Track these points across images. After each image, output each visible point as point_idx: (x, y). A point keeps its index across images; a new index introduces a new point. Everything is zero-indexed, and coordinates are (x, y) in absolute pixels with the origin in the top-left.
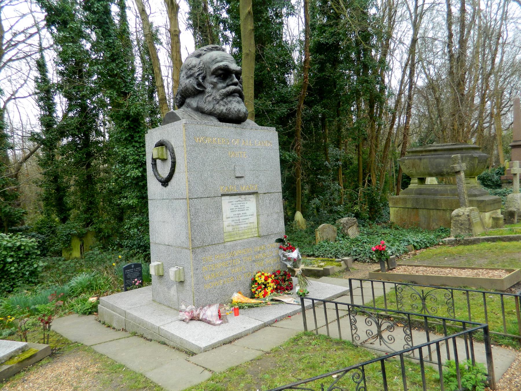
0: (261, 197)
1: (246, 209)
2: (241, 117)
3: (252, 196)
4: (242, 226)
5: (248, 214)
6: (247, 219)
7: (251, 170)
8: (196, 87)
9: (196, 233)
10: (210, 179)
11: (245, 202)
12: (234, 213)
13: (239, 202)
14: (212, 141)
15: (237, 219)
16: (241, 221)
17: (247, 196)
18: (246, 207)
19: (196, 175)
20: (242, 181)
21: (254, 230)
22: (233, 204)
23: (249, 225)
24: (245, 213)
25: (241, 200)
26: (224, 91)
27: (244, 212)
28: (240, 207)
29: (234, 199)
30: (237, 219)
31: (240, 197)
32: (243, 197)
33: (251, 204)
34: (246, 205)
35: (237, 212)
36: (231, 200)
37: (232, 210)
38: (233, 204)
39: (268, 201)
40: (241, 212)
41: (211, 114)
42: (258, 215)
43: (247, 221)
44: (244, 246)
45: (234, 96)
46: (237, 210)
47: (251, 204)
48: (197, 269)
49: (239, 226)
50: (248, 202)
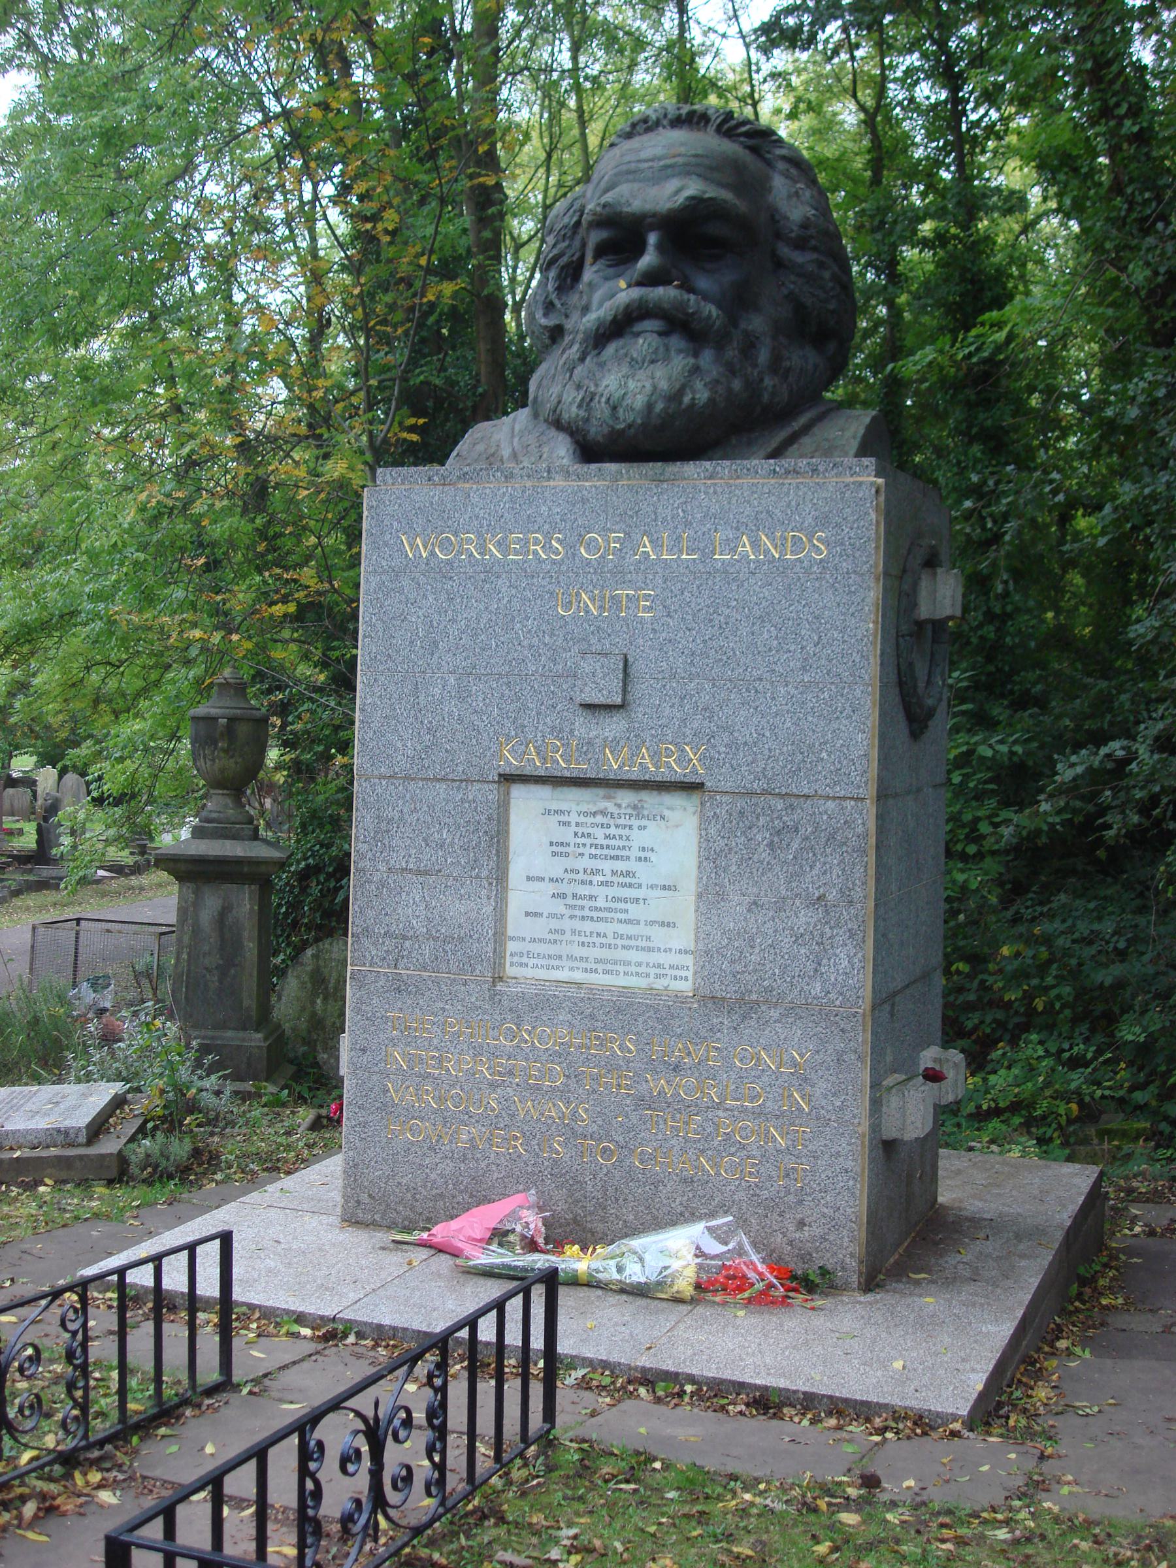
0: (722, 812)
1: (635, 853)
7: (673, 676)
8: (539, 315)
9: (371, 913)
10: (452, 707)
11: (636, 823)
12: (569, 863)
13: (599, 819)
14: (483, 550)
15: (584, 890)
16: (601, 903)
17: (650, 800)
18: (635, 845)
19: (393, 687)
20: (613, 726)
24: (628, 874)
26: (591, 319)
27: (620, 866)
28: (601, 841)
29: (574, 801)
30: (584, 890)
31: (608, 798)
32: (626, 798)
33: (671, 840)
34: (639, 838)
35: (584, 863)
36: (554, 806)
37: (559, 849)
40: (607, 866)
41: (558, 424)
43: (634, 911)
44: (592, 1017)
45: (638, 335)
46: (587, 851)
48: (364, 1050)
49: (588, 926)
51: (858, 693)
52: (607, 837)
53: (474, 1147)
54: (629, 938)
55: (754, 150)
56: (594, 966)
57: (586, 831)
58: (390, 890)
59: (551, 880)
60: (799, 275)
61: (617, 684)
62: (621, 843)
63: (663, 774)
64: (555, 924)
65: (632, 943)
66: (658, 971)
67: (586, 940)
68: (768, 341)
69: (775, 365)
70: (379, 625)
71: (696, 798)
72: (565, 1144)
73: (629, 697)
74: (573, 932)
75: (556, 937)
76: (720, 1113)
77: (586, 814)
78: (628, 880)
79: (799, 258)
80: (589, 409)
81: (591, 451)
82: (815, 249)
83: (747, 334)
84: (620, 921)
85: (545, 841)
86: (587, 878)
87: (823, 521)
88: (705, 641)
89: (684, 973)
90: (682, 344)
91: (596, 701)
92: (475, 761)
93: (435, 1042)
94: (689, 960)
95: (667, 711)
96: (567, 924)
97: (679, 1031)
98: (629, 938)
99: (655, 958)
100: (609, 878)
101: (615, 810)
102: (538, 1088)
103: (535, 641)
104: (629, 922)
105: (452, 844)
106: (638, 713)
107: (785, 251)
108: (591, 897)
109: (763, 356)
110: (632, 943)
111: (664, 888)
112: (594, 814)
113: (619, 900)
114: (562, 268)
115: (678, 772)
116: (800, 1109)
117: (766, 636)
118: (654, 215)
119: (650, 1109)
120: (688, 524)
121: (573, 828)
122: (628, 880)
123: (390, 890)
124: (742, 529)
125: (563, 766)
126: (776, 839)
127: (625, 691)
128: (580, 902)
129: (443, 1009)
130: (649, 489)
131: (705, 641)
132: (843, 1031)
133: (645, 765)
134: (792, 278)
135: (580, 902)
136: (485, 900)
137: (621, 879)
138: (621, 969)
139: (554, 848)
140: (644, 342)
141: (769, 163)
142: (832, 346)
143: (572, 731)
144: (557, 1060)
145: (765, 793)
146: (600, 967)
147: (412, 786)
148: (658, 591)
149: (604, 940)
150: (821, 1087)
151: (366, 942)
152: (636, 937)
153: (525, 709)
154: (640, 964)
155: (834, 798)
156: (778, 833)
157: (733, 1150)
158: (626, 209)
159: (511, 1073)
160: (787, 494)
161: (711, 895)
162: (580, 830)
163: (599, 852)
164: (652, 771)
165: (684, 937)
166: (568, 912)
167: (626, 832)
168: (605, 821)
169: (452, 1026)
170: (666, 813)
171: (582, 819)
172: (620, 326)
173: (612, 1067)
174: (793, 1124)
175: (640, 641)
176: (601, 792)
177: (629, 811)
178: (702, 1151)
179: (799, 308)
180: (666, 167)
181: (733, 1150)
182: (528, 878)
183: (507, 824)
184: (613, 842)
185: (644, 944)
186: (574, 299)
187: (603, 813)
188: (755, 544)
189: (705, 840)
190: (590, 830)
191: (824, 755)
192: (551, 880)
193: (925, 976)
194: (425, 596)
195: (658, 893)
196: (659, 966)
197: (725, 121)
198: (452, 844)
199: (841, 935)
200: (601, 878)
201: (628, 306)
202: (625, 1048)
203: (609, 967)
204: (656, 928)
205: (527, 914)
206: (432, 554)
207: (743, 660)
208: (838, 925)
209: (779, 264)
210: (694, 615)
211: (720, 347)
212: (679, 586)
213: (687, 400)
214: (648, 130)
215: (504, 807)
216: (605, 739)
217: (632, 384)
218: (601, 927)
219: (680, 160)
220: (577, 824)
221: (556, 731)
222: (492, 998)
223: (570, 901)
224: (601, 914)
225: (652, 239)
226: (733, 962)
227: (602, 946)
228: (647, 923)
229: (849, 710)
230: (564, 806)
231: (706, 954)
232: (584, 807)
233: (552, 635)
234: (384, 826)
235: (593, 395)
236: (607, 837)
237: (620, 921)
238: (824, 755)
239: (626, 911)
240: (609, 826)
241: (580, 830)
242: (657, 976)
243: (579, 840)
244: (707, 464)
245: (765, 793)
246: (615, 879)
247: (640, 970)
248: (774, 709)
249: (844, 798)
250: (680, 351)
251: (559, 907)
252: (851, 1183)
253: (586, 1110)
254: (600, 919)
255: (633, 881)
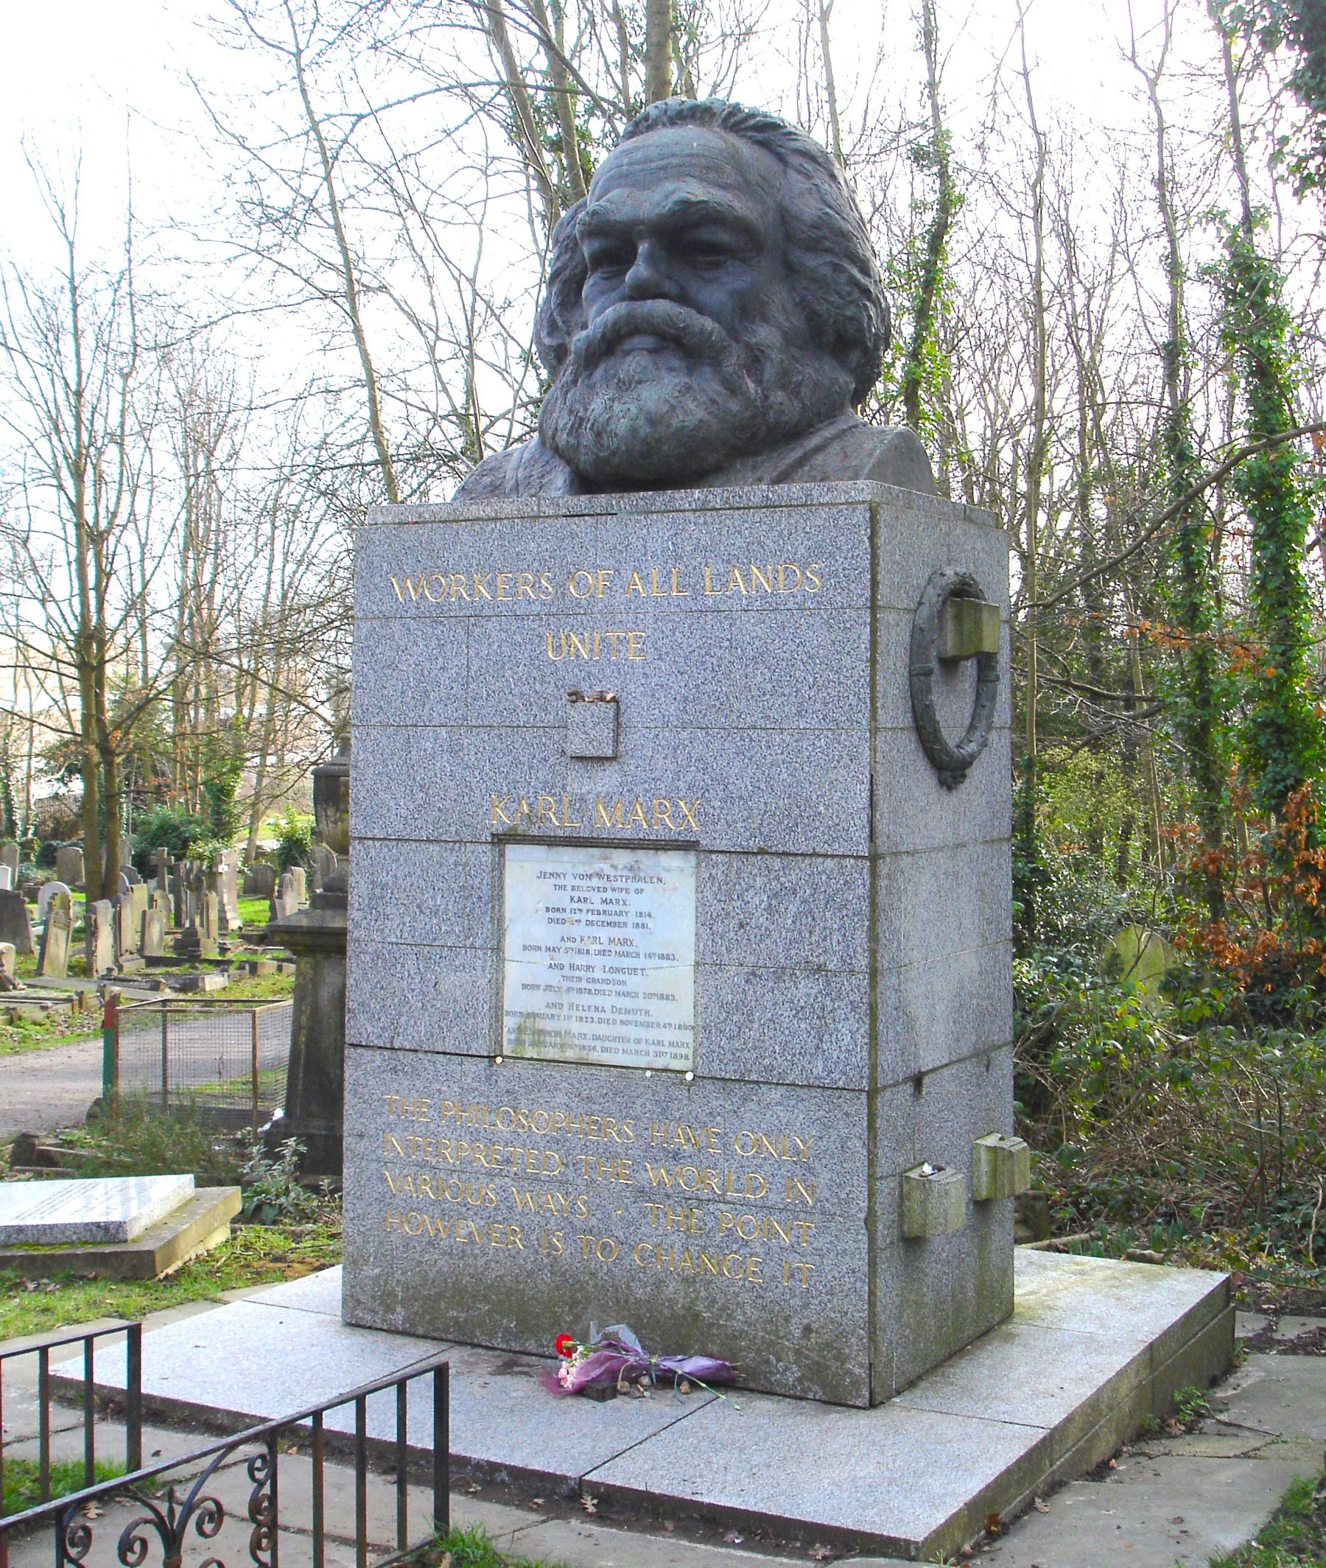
1: (632, 919)
2: (606, 461)
3: (672, 861)
4: (607, 1002)
5: (641, 950)
6: (634, 971)
10: (444, 762)
11: (632, 886)
12: (566, 930)
13: (595, 882)
14: (471, 588)
15: (581, 961)
16: (598, 974)
18: (632, 909)
19: (385, 741)
20: (607, 779)
21: (668, 1035)
22: (563, 888)
23: (640, 1003)
24: (625, 942)
25: (607, 870)
27: (617, 933)
30: (581, 961)
31: (606, 858)
32: (622, 858)
34: (637, 903)
37: (555, 915)
38: (563, 888)
39: (758, 900)
40: (604, 933)
42: (697, 963)
43: (634, 982)
44: (589, 1099)
45: (627, 353)
46: (583, 917)
47: (670, 901)
48: (361, 1136)
49: (585, 1000)
50: (648, 888)
51: (855, 740)
52: (605, 901)
53: (473, 1242)
54: (627, 1012)
55: (764, 144)
56: (592, 1043)
57: (582, 895)
58: (384, 960)
59: (548, 949)
60: (813, 280)
61: (608, 734)
62: (618, 908)
63: (657, 833)
64: (551, 997)
65: (631, 1017)
66: (658, 1049)
67: (584, 1014)
68: (776, 355)
69: (784, 380)
70: (371, 676)
71: (692, 857)
72: (564, 1239)
73: (621, 748)
74: (571, 1005)
75: (553, 1011)
76: (721, 1206)
77: (582, 877)
78: (626, 949)
79: (811, 261)
80: (578, 437)
81: (585, 483)
82: (828, 250)
83: (748, 346)
84: (618, 994)
85: (542, 906)
86: (582, 946)
87: (816, 552)
88: (697, 686)
89: (684, 1051)
90: (675, 362)
91: (587, 754)
92: (468, 820)
93: (432, 1126)
94: (688, 1037)
95: (661, 762)
96: (565, 999)
97: (677, 1115)
98: (627, 1012)
99: (652, 1034)
100: (606, 947)
101: (612, 872)
102: (536, 1179)
103: (526, 689)
104: (627, 994)
105: (446, 910)
106: (631, 764)
107: (796, 255)
108: (588, 967)
109: (769, 373)
110: (631, 1017)
111: (662, 957)
112: (590, 877)
113: (618, 970)
114: (565, 283)
115: (669, 827)
116: (805, 1203)
117: (759, 679)
118: (642, 222)
119: (650, 1201)
120: (678, 558)
121: (569, 892)
122: (626, 949)
123: (384, 960)
124: (734, 562)
125: (555, 825)
126: (774, 902)
127: (616, 741)
128: (577, 973)
129: (440, 1091)
130: (638, 521)
131: (697, 686)
132: (847, 1114)
133: (638, 823)
134: (805, 283)
135: (577, 973)
136: (479, 973)
137: (619, 948)
138: (620, 1046)
139: (551, 915)
140: (633, 363)
141: (781, 158)
142: (855, 357)
143: (564, 787)
144: (555, 1146)
145: (762, 852)
146: (599, 1044)
147: (405, 847)
148: (649, 632)
149: (602, 1015)
150: (824, 1177)
151: (362, 1017)
152: (634, 1012)
153: (517, 763)
154: (638, 1041)
155: (833, 856)
156: (776, 895)
157: (735, 1247)
158: (618, 217)
159: (508, 1161)
160: (779, 523)
161: (707, 965)
162: (576, 894)
163: (595, 918)
164: (644, 831)
165: (684, 1010)
166: (566, 984)
167: (623, 895)
168: (601, 883)
169: (447, 1109)
170: (663, 875)
171: (578, 882)
172: (609, 345)
173: (610, 1155)
174: (796, 1218)
175: (632, 686)
176: (595, 851)
177: (626, 873)
178: (704, 1248)
179: (812, 317)
180: (659, 169)
181: (735, 1247)
182: (525, 948)
183: (502, 889)
184: (609, 907)
185: (643, 1018)
186: (576, 317)
187: (599, 875)
188: (747, 577)
189: (701, 903)
190: (587, 895)
191: (822, 808)
192: (548, 949)
193: (983, 1056)
194: (416, 643)
195: (656, 962)
196: (660, 1043)
197: (730, 114)
198: (446, 910)
199: (842, 1007)
200: (598, 947)
201: (615, 324)
202: (622, 1134)
203: (607, 1044)
204: (655, 1001)
205: (525, 986)
206: (423, 597)
207: (737, 705)
208: (839, 998)
209: (791, 270)
210: (686, 658)
211: (716, 363)
212: (670, 626)
213: (675, 423)
214: (649, 128)
215: (499, 868)
216: (598, 795)
217: (617, 407)
218: (597, 1000)
219: (675, 161)
220: (573, 888)
221: (548, 787)
222: (488, 1079)
223: (567, 972)
224: (598, 986)
225: (643, 248)
226: (731, 1038)
227: (600, 1021)
228: (648, 996)
229: (846, 760)
230: (559, 869)
231: (703, 1029)
232: (581, 870)
233: (543, 682)
234: (378, 891)
235: (582, 419)
236: (605, 901)
237: (618, 994)
238: (822, 808)
239: (624, 983)
240: (605, 890)
241: (576, 894)
242: (657, 1054)
243: (576, 906)
244: (697, 493)
245: (762, 852)
246: (613, 948)
247: (638, 1047)
248: (769, 759)
249: (844, 856)
250: (671, 369)
251: (554, 978)
252: (858, 1285)
253: (585, 1203)
254: (598, 992)
255: (631, 949)
